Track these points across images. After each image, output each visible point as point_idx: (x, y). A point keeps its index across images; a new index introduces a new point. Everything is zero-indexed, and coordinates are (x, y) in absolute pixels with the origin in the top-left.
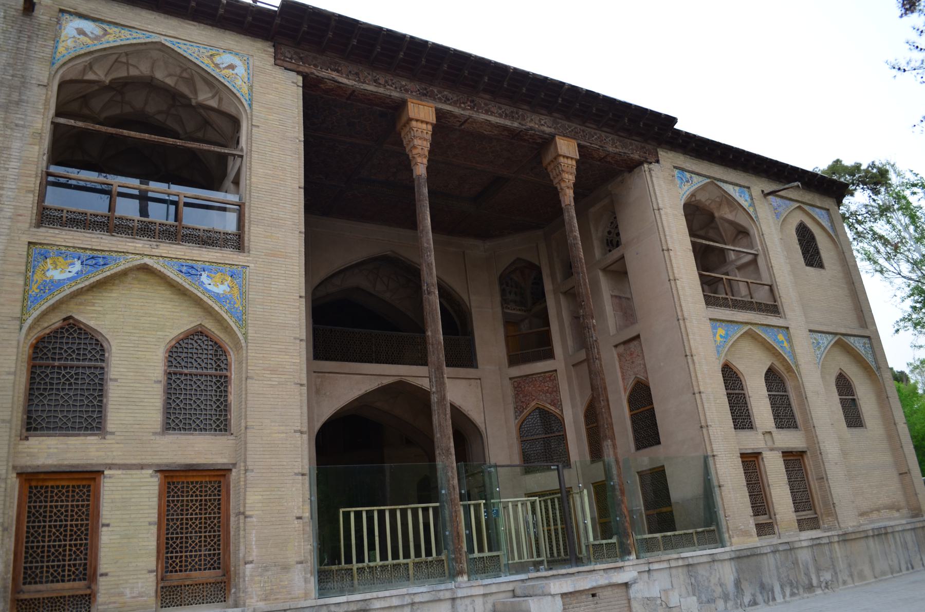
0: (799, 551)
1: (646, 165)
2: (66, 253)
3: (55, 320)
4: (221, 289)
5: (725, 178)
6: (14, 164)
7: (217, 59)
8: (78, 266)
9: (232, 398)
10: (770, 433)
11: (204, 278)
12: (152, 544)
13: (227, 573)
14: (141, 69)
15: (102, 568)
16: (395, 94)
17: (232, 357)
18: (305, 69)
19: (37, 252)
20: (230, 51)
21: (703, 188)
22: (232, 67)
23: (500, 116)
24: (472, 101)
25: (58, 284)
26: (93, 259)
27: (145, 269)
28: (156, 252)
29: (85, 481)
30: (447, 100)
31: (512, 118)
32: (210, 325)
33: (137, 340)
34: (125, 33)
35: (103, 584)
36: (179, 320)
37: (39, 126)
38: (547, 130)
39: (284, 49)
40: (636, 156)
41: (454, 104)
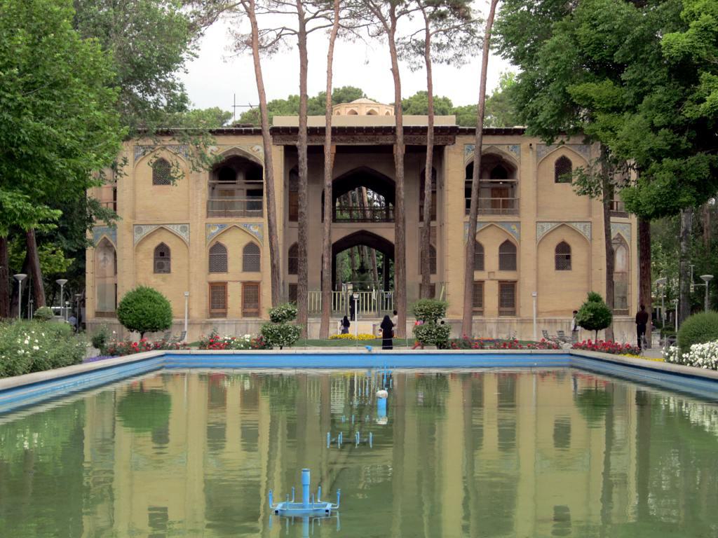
0: (488, 324)
1: (447, 147)
2: (215, 225)
3: (214, 243)
4: (256, 230)
5: (501, 143)
6: (199, 201)
7: (253, 149)
8: (218, 228)
9: (261, 262)
10: (494, 272)
11: (251, 228)
12: (240, 301)
13: (259, 310)
14: (233, 153)
15: (229, 306)
16: (319, 144)
17: (261, 250)
18: (285, 144)
19: (208, 226)
20: (257, 144)
21: (488, 148)
22: (258, 150)
23: (366, 141)
24: (354, 138)
25: (213, 234)
26: (222, 226)
27: (235, 226)
28: (239, 221)
29: (223, 285)
30: (341, 140)
31: (372, 140)
32: (254, 241)
33: (234, 247)
34: (225, 147)
35: (229, 310)
36: (245, 240)
37: (204, 187)
38: (390, 142)
39: (277, 137)
40: (440, 144)
41: (345, 141)
